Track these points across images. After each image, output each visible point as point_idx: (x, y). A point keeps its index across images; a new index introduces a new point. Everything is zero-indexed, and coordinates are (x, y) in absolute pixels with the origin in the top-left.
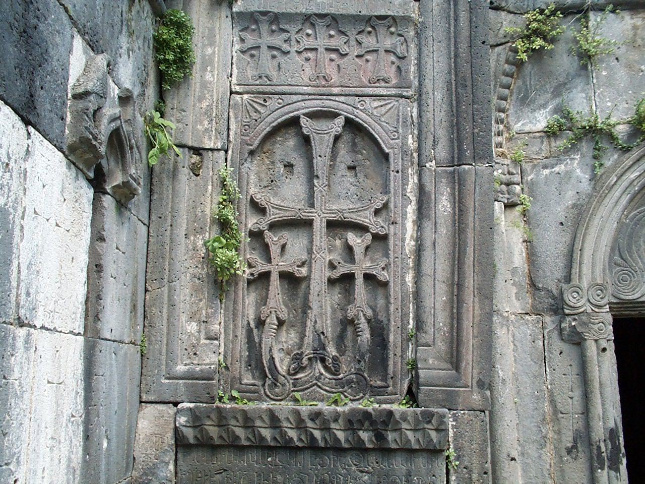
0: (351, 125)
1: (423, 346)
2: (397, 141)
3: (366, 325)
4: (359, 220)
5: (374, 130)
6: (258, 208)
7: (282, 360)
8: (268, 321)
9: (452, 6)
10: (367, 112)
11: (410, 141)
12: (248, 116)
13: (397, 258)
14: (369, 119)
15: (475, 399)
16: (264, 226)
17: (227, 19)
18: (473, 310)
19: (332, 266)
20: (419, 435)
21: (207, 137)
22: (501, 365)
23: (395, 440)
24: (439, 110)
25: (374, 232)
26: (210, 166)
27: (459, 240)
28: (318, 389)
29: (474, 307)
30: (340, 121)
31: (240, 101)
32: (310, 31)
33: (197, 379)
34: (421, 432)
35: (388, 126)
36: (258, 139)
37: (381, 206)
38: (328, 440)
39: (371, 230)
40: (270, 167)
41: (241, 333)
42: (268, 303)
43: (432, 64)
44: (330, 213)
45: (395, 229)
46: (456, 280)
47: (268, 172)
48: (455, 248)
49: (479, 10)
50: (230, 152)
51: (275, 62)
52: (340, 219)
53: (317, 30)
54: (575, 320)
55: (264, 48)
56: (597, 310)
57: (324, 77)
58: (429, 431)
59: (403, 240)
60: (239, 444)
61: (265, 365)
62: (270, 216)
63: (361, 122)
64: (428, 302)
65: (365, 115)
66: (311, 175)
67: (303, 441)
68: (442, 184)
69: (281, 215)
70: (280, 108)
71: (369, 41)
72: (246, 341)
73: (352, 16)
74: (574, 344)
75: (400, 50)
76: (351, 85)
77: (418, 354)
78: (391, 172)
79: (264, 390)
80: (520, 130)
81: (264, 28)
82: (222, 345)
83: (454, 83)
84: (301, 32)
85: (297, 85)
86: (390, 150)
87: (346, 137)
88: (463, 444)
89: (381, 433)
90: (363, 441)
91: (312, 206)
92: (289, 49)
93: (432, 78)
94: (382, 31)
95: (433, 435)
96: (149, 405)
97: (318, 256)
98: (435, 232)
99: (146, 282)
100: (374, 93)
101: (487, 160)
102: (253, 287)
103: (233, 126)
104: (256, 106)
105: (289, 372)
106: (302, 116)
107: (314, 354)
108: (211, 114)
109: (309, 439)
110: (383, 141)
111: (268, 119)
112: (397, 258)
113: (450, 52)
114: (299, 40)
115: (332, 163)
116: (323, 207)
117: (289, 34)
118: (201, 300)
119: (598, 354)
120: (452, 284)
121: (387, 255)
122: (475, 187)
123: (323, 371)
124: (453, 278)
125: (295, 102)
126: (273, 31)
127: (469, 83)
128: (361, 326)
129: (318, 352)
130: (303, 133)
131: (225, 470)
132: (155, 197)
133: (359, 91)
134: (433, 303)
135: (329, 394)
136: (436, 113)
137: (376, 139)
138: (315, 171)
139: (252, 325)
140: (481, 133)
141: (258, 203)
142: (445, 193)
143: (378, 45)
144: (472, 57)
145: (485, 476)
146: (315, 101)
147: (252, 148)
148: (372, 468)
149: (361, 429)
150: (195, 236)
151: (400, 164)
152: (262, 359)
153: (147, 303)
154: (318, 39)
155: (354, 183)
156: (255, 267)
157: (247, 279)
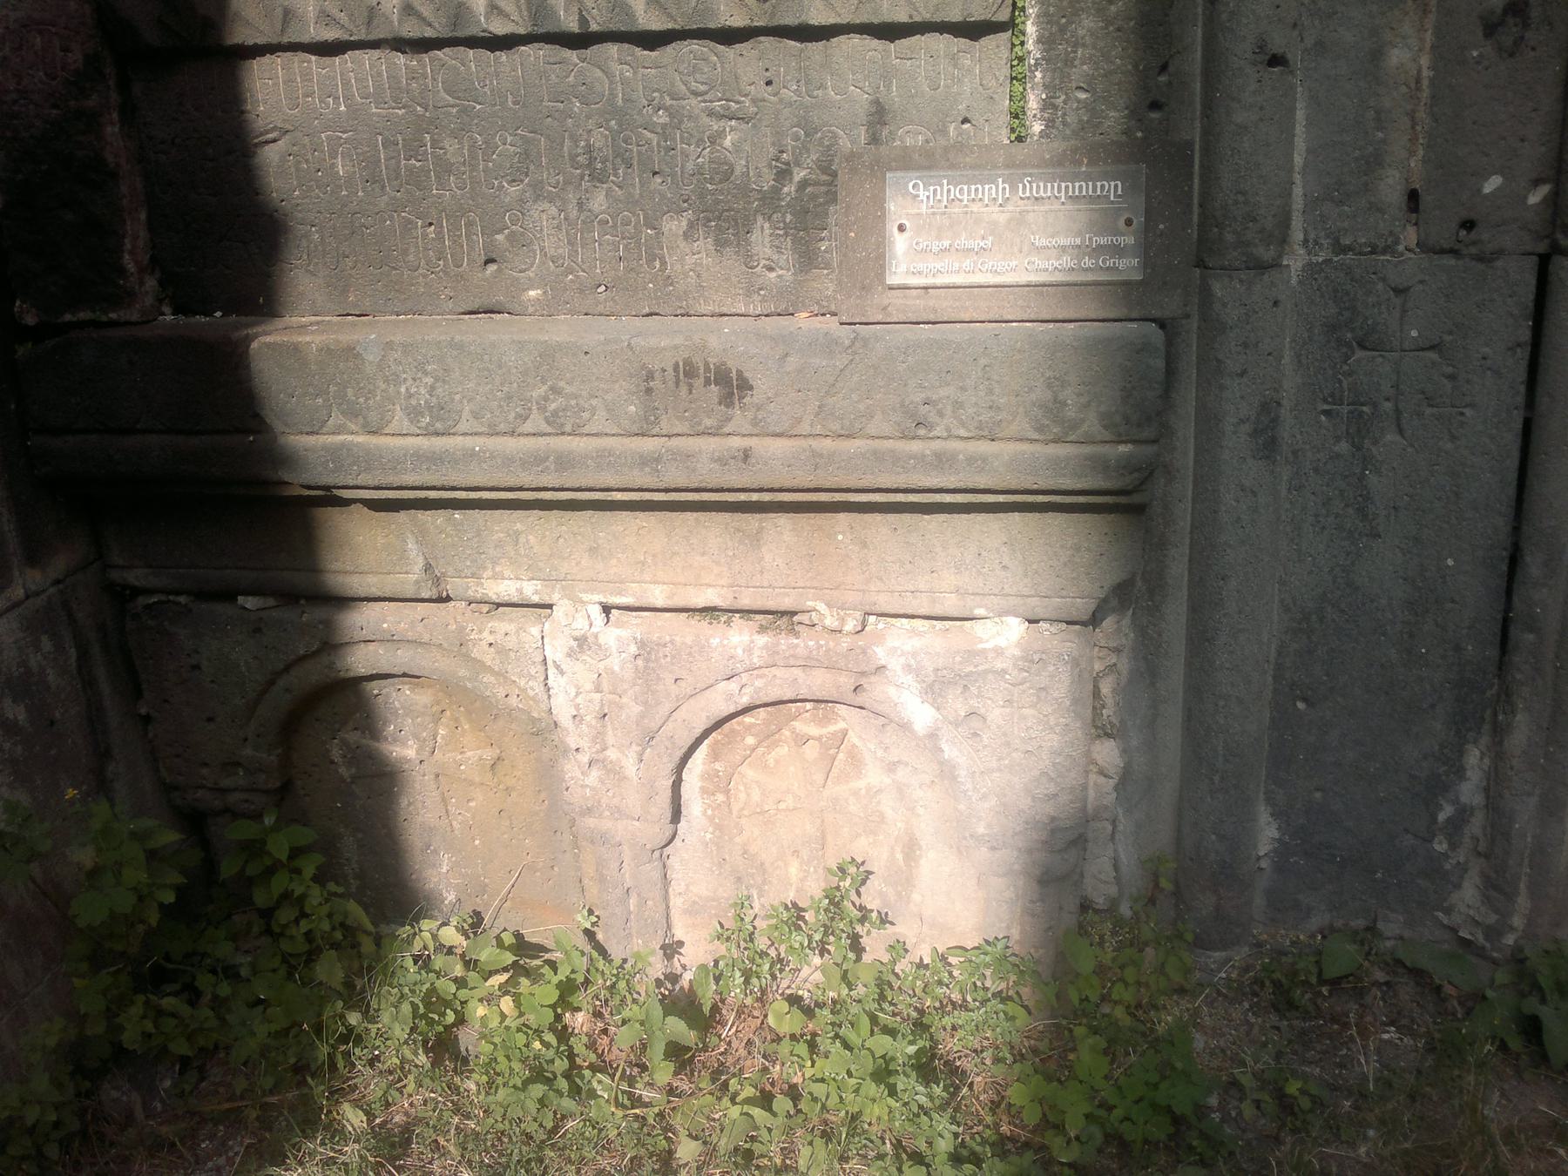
67: (507, 16)
148: (754, 101)
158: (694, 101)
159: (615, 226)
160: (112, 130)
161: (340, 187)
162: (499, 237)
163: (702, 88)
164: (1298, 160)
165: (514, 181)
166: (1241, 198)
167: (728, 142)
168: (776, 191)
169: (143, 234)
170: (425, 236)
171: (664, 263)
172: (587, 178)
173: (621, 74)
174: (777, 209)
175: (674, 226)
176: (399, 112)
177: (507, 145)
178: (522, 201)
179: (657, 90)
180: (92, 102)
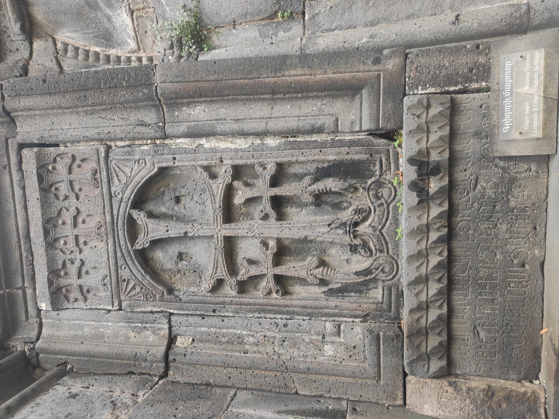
1: (337, 126)
2: (147, 160)
3: (320, 183)
4: (221, 194)
5: (140, 182)
6: (219, 284)
8: (320, 277)
9: (19, 113)
10: (124, 189)
11: (145, 147)
12: (139, 295)
13: (253, 156)
16: (232, 281)
17: (60, 314)
18: (298, 76)
19: (266, 217)
20: (434, 128)
21: (159, 332)
22: (355, 41)
23: (440, 153)
24: (113, 121)
25: (230, 179)
26: (184, 329)
27: (229, 95)
28: (385, 228)
29: (294, 76)
30: (135, 214)
31: (127, 302)
32: (62, 242)
34: (430, 125)
36: (157, 286)
37: (206, 173)
38: (440, 224)
39: (230, 182)
40: (182, 273)
41: (334, 302)
42: (303, 277)
43: (73, 130)
44: (217, 221)
46: (268, 96)
47: (187, 275)
48: (238, 100)
49: (17, 87)
50: (171, 311)
51: (92, 271)
52: (222, 211)
53: (60, 236)
55: (80, 282)
58: (429, 116)
59: (236, 150)
60: (446, 315)
61: (362, 280)
62: (223, 276)
63: (133, 194)
64: (293, 124)
65: (127, 191)
66: (185, 237)
68: (180, 116)
69: (222, 265)
70: (129, 267)
71: (64, 189)
72: (340, 294)
73: (42, 206)
75: (67, 160)
76: (102, 204)
77: (346, 130)
78: (175, 165)
79: (387, 280)
80: (134, 40)
81: (63, 282)
83: (85, 108)
84: (64, 250)
85: (108, 252)
86: (156, 166)
87: (151, 207)
88: (444, 75)
90: (441, 188)
91: (212, 237)
92: (78, 261)
93: (85, 129)
94: (53, 178)
95: (433, 111)
96: (408, 402)
97: (256, 231)
98: (225, 120)
100: (106, 183)
102: (291, 289)
103: (149, 309)
104: (129, 289)
105: (369, 256)
106: (134, 248)
107: (350, 233)
109: (439, 245)
110: (149, 173)
112: (253, 156)
113: (60, 113)
114: (70, 251)
115: (174, 219)
116: (212, 227)
117: (66, 260)
118: (303, 340)
120: (274, 100)
121: (252, 166)
122: (177, 82)
123: (367, 223)
124: (267, 99)
125: (123, 254)
126: (66, 274)
127: (82, 94)
128: (320, 189)
129: (348, 229)
130: (148, 247)
131: (475, 327)
132: (211, 381)
133: (107, 197)
134: (293, 118)
135: (390, 218)
136: (116, 125)
137: (147, 180)
138: (181, 235)
139: (325, 289)
141: (213, 287)
142: (188, 112)
143: (66, 181)
144: (59, 92)
145: (481, 47)
146: (120, 236)
147: (165, 292)
148: (471, 176)
150: (245, 344)
151: (167, 156)
152: (357, 282)
153: (308, 394)
154: (67, 234)
155: (191, 197)
156: (270, 289)
157: (282, 296)
158: (470, 195)
159: (512, 222)
161: (495, 313)
163: (466, 191)
165: (495, 255)
166: (504, 20)
168: (503, 168)
169: (509, 382)
170: (513, 287)
171: (527, 207)
172: (495, 230)
173: (460, 217)
174: (509, 168)
175: (513, 204)
176: (470, 289)
177: (483, 255)
179: (466, 205)
180: (464, 388)
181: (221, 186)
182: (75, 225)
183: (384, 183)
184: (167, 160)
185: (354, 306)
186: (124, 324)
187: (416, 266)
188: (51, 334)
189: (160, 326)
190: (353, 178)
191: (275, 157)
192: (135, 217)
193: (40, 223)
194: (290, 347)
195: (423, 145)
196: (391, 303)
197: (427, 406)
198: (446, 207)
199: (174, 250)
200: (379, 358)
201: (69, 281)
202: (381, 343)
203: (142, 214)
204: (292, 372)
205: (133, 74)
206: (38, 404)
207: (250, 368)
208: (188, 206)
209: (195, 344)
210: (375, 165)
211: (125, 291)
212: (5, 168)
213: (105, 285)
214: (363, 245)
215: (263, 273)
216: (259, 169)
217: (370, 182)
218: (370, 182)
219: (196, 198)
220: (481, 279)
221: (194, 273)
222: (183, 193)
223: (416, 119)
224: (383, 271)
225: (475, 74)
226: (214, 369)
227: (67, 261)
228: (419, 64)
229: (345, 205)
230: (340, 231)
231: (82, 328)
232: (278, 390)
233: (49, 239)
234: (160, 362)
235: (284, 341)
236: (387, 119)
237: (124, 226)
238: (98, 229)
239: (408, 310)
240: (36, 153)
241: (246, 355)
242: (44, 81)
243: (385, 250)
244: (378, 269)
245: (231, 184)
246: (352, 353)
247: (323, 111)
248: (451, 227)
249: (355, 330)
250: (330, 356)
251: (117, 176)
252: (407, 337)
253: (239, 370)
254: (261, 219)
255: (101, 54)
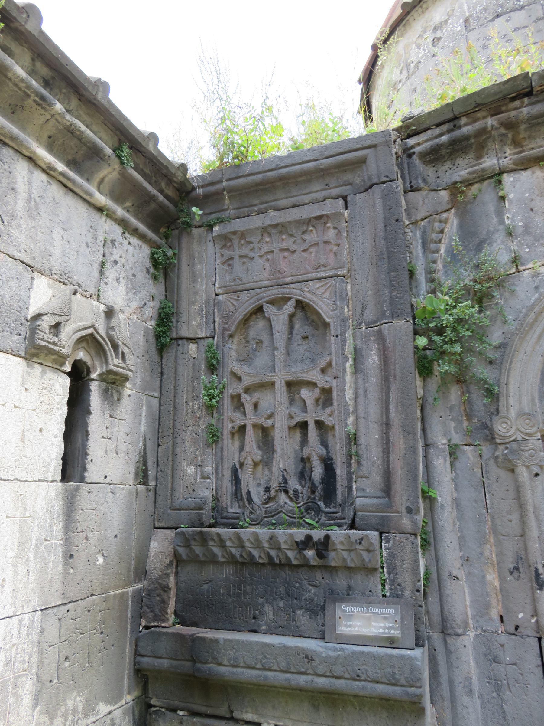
0: (300, 305)
1: (362, 478)
2: (335, 312)
3: (319, 462)
7: (259, 493)
8: (246, 462)
11: (346, 310)
14: (314, 298)
15: (404, 523)
21: (199, 330)
23: (334, 559)
32: (268, 240)
33: (192, 509)
35: (328, 301)
38: (281, 557)
40: (247, 345)
41: (227, 474)
44: (287, 375)
45: (337, 382)
46: (384, 420)
49: (392, 195)
50: (216, 338)
54: (507, 448)
55: (237, 258)
56: (527, 438)
57: (279, 271)
59: (344, 390)
63: (307, 301)
68: (371, 341)
70: (248, 300)
74: (509, 470)
81: (236, 242)
82: (214, 482)
85: (260, 281)
87: (300, 314)
89: (321, 552)
91: (275, 372)
95: (365, 554)
99: (158, 439)
101: (404, 317)
103: (217, 320)
106: (264, 304)
107: (279, 487)
108: (202, 313)
110: (325, 313)
111: (240, 310)
115: (290, 336)
118: (197, 450)
119: (531, 479)
123: (288, 501)
124: (382, 419)
127: (385, 256)
131: (210, 581)
132: (165, 377)
133: (304, 277)
135: (291, 519)
139: (237, 466)
140: (398, 295)
142: (373, 349)
145: (418, 593)
146: (273, 291)
147: (230, 332)
148: (320, 582)
149: (305, 549)
150: (193, 402)
151: (339, 329)
153: (159, 455)
158: (305, 581)
160: (172, 578)
162: (257, 612)
164: (468, 603)
167: (313, 592)
169: (174, 604)
175: (298, 612)
177: (261, 588)
178: (263, 603)
180: (169, 571)
181: (315, 378)
182: (282, 250)
183: (318, 516)
184: (336, 330)
185: (224, 490)
186: (204, 299)
187: (251, 539)
188: (195, 237)
189: (204, 329)
190: (323, 489)
191: (339, 424)
192: (289, 303)
193: (282, 220)
194: (192, 439)
195: (339, 547)
196: (227, 519)
197: (156, 544)
198: (295, 562)
199: (265, 337)
200: (187, 510)
201: (237, 248)
202: (197, 511)
203: (291, 309)
204: (174, 442)
205: (402, 301)
206: (141, 247)
207: (175, 407)
208: (300, 347)
209: (192, 360)
210: (335, 507)
211: (231, 298)
212: (327, 185)
213: (235, 280)
214: (270, 498)
215: (247, 415)
216: (328, 410)
217: (321, 504)
218: (321, 504)
219: (307, 354)
220: (244, 587)
221: (246, 355)
222: (310, 342)
223: (358, 541)
224: (251, 513)
225: (396, 588)
226: (173, 379)
227: (252, 245)
228: (405, 544)
229: (303, 482)
230: (281, 479)
231: (200, 263)
232: (160, 431)
233: (269, 229)
234: (177, 334)
235: (196, 434)
236: (363, 518)
237: (282, 294)
238: (279, 271)
239: (219, 532)
240: (340, 212)
241: (185, 403)
242: (397, 220)
243: (267, 515)
244: (253, 509)
245: (317, 387)
246: (189, 488)
247: (373, 466)
248: (281, 565)
249: (206, 491)
250: (187, 471)
251: (322, 286)
252: (201, 532)
253: (172, 398)
254: (289, 413)
255: (437, 255)
